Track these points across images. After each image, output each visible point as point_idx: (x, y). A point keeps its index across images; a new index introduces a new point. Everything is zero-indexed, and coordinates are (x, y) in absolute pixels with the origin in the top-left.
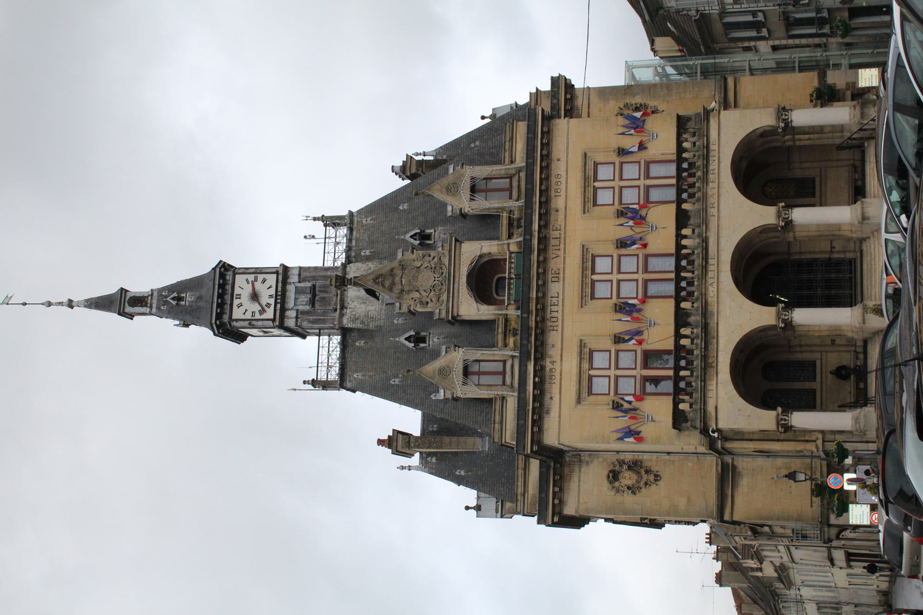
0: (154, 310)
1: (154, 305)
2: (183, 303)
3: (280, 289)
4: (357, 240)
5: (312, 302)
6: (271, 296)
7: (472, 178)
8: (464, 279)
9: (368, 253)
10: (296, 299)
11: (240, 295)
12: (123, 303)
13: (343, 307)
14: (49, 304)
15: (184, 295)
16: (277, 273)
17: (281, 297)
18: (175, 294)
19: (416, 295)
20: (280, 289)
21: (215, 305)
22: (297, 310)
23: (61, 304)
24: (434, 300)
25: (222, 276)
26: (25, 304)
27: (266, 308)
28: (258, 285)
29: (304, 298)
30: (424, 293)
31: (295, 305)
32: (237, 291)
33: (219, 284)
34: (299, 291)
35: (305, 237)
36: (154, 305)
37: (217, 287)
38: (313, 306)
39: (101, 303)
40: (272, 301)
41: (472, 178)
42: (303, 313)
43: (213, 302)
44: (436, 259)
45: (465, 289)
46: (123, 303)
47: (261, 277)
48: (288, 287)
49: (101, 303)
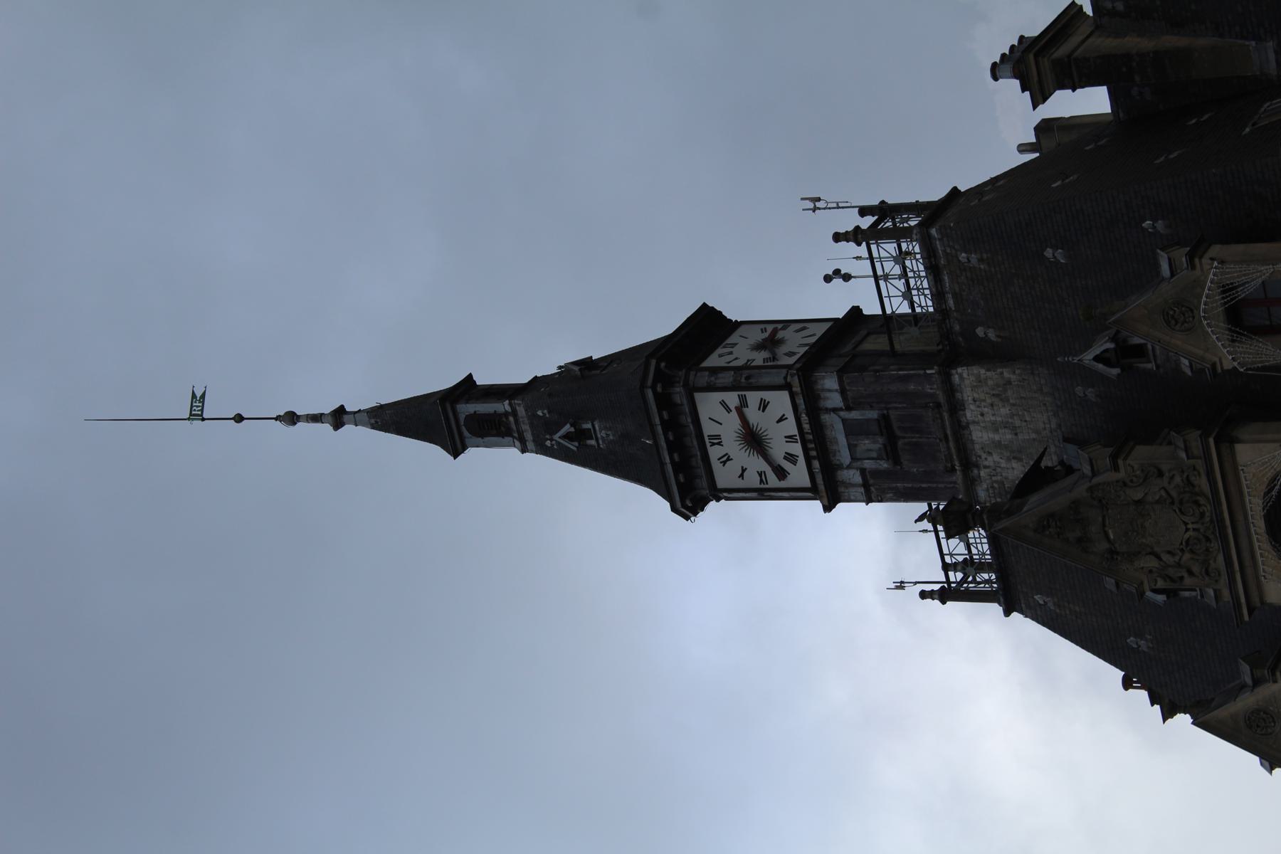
0: (530, 445)
1: (528, 436)
2: (593, 442)
3: (806, 427)
4: (955, 296)
5: (891, 451)
6: (790, 438)
7: (1227, 289)
8: (1258, 525)
9: (992, 335)
10: (852, 447)
11: (718, 437)
12: (452, 417)
13: (968, 464)
14: (291, 418)
15: (589, 426)
16: (787, 386)
17: (815, 442)
18: (567, 428)
19: (1152, 563)
20: (806, 427)
21: (669, 468)
22: (863, 472)
23: (316, 418)
24: (1196, 569)
25: (664, 402)
26: (239, 418)
27: (787, 465)
28: (752, 414)
29: (871, 445)
30: (1165, 557)
31: (854, 459)
32: (708, 429)
33: (663, 422)
34: (852, 430)
35: (828, 279)
36: (528, 436)
37: (659, 429)
38: (897, 461)
39: (403, 418)
40: (797, 449)
41: (1227, 289)
42: (877, 474)
43: (662, 464)
44: (1178, 479)
45: (1267, 546)
46: (452, 417)
47: (753, 397)
48: (827, 418)
49: (403, 418)
